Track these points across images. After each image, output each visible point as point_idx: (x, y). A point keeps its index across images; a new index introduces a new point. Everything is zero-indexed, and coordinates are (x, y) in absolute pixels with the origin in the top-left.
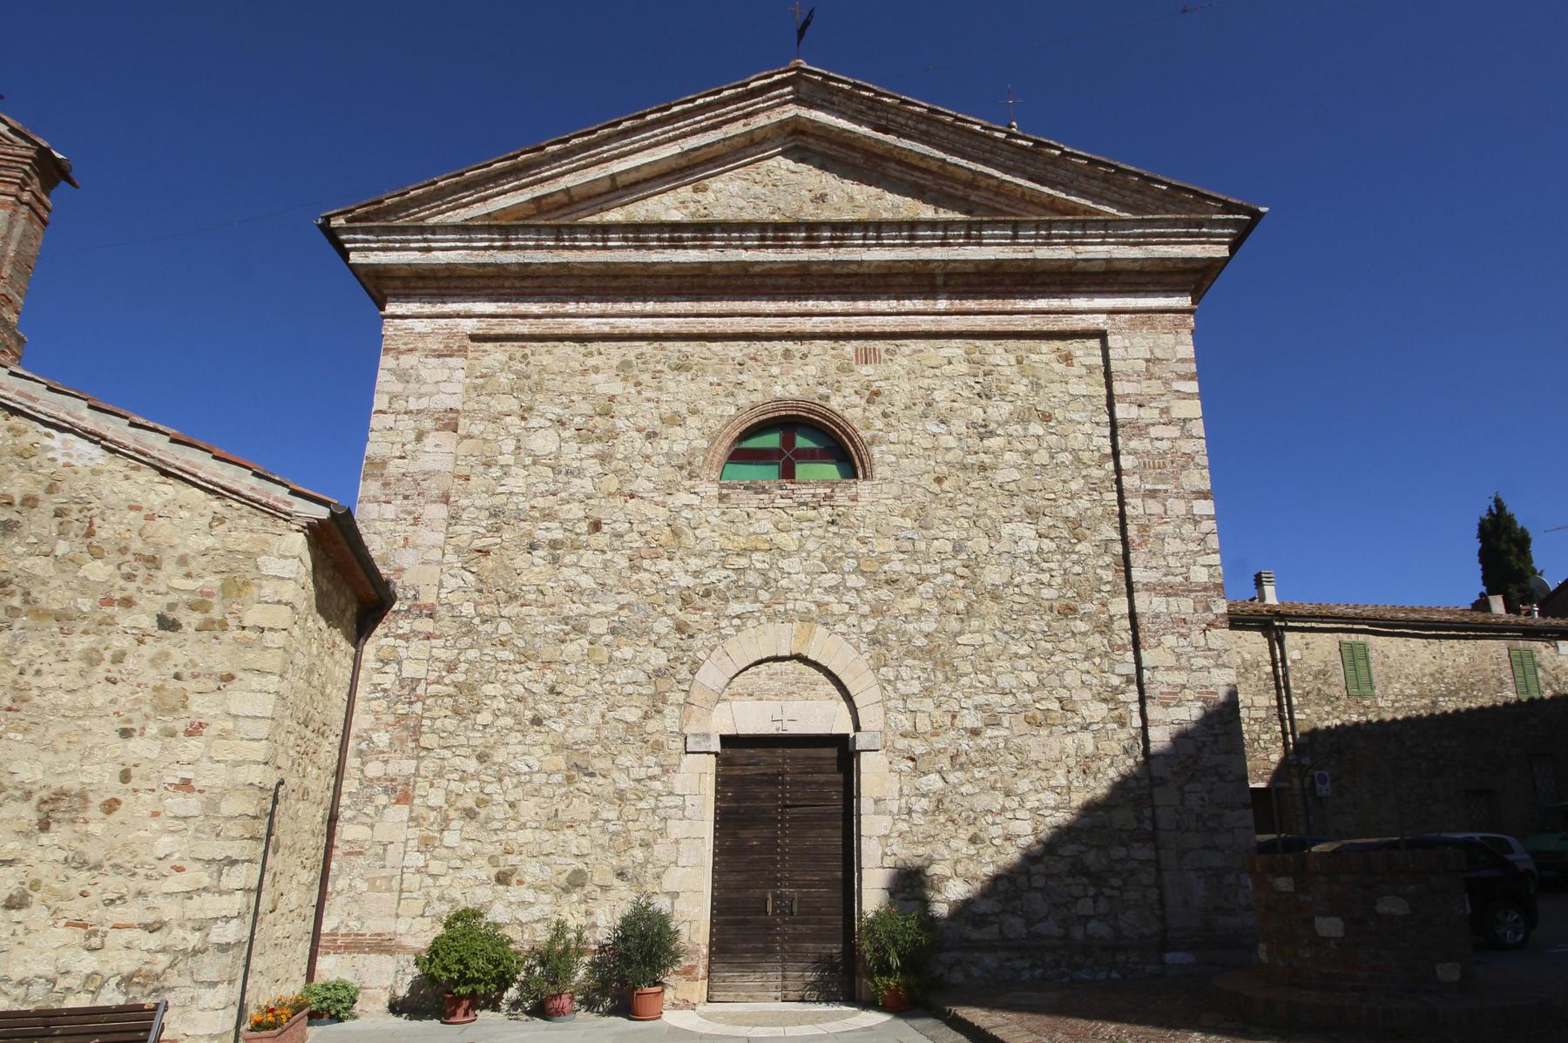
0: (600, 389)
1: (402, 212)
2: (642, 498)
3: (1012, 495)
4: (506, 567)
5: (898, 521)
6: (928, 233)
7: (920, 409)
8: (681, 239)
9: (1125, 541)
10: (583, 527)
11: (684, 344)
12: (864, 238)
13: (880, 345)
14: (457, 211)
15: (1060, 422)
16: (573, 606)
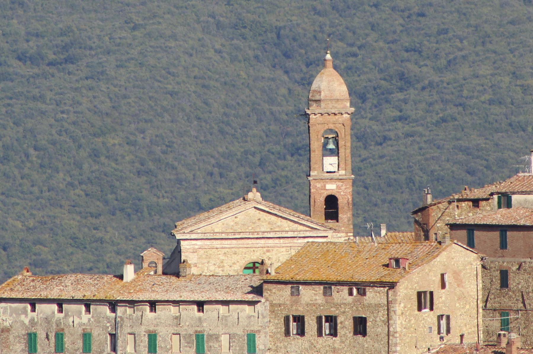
0: (221, 258)
7: (278, 261)
13: (270, 249)
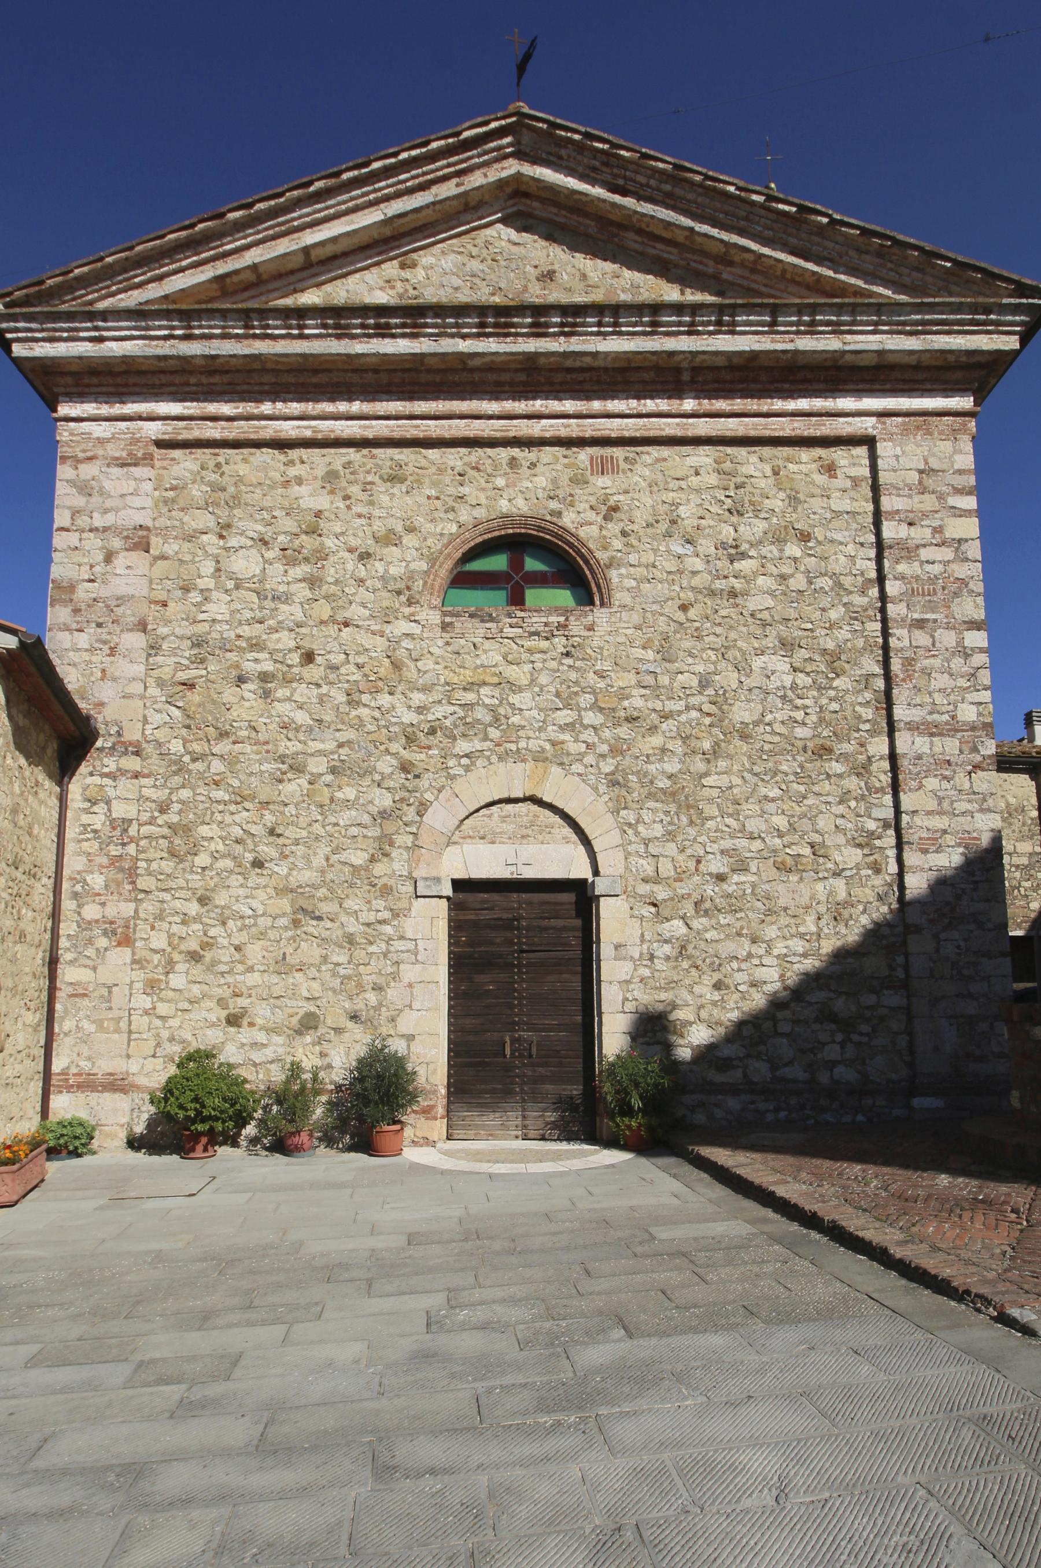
1: (66, 294)
2: (357, 626)
3: (765, 625)
4: (214, 702)
5: (639, 653)
6: (674, 318)
7: (663, 527)
8: (388, 326)
9: (888, 676)
10: (295, 658)
11: (397, 450)
12: (600, 324)
13: (618, 452)
14: (130, 293)
15: (820, 543)
16: (289, 744)
